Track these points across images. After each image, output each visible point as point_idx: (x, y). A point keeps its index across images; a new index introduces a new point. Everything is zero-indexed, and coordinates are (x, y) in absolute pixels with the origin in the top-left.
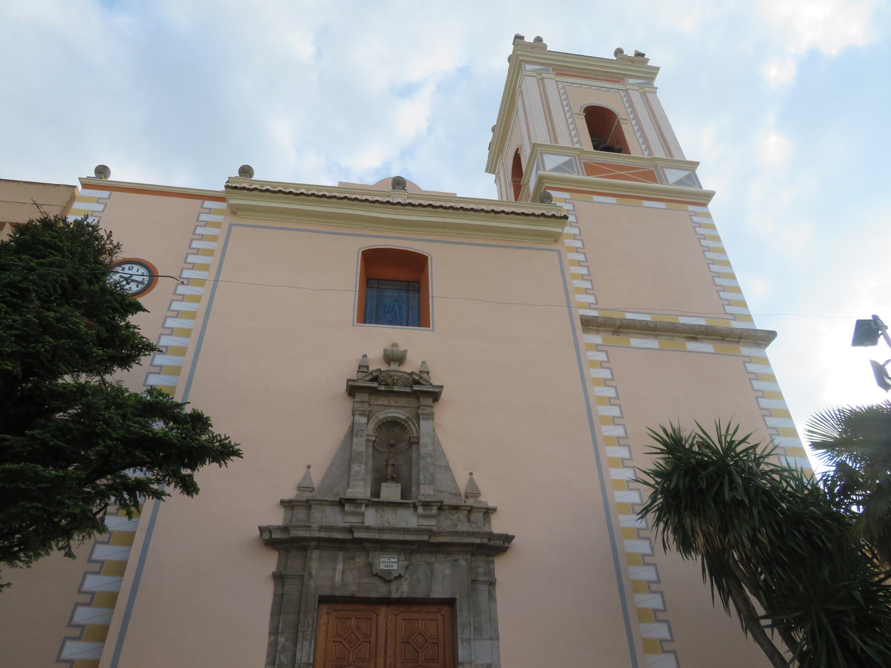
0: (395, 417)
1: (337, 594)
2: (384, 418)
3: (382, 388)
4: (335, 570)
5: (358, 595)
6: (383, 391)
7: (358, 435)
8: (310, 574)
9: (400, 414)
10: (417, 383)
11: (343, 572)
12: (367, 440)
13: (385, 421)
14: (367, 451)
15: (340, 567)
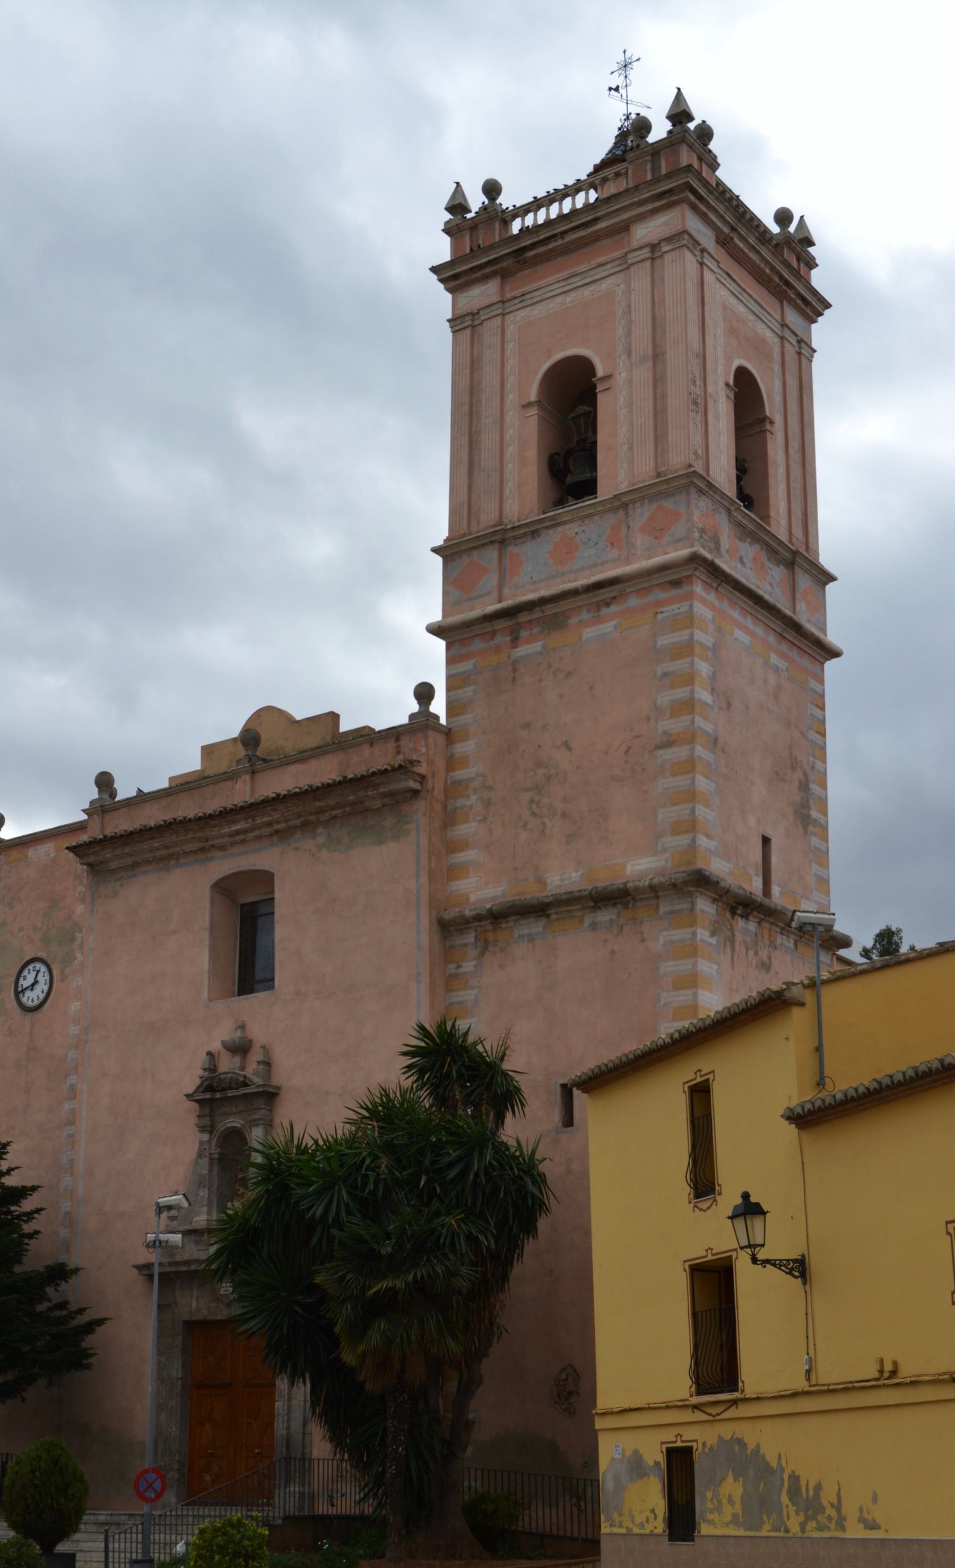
0: (234, 1127)
1: (194, 1318)
2: (225, 1130)
3: (218, 1096)
4: (192, 1296)
5: (209, 1318)
6: (218, 1098)
7: (202, 1156)
8: (175, 1302)
9: (235, 1122)
10: (246, 1085)
11: (198, 1298)
12: (211, 1159)
13: (227, 1132)
14: (210, 1170)
15: (195, 1293)
